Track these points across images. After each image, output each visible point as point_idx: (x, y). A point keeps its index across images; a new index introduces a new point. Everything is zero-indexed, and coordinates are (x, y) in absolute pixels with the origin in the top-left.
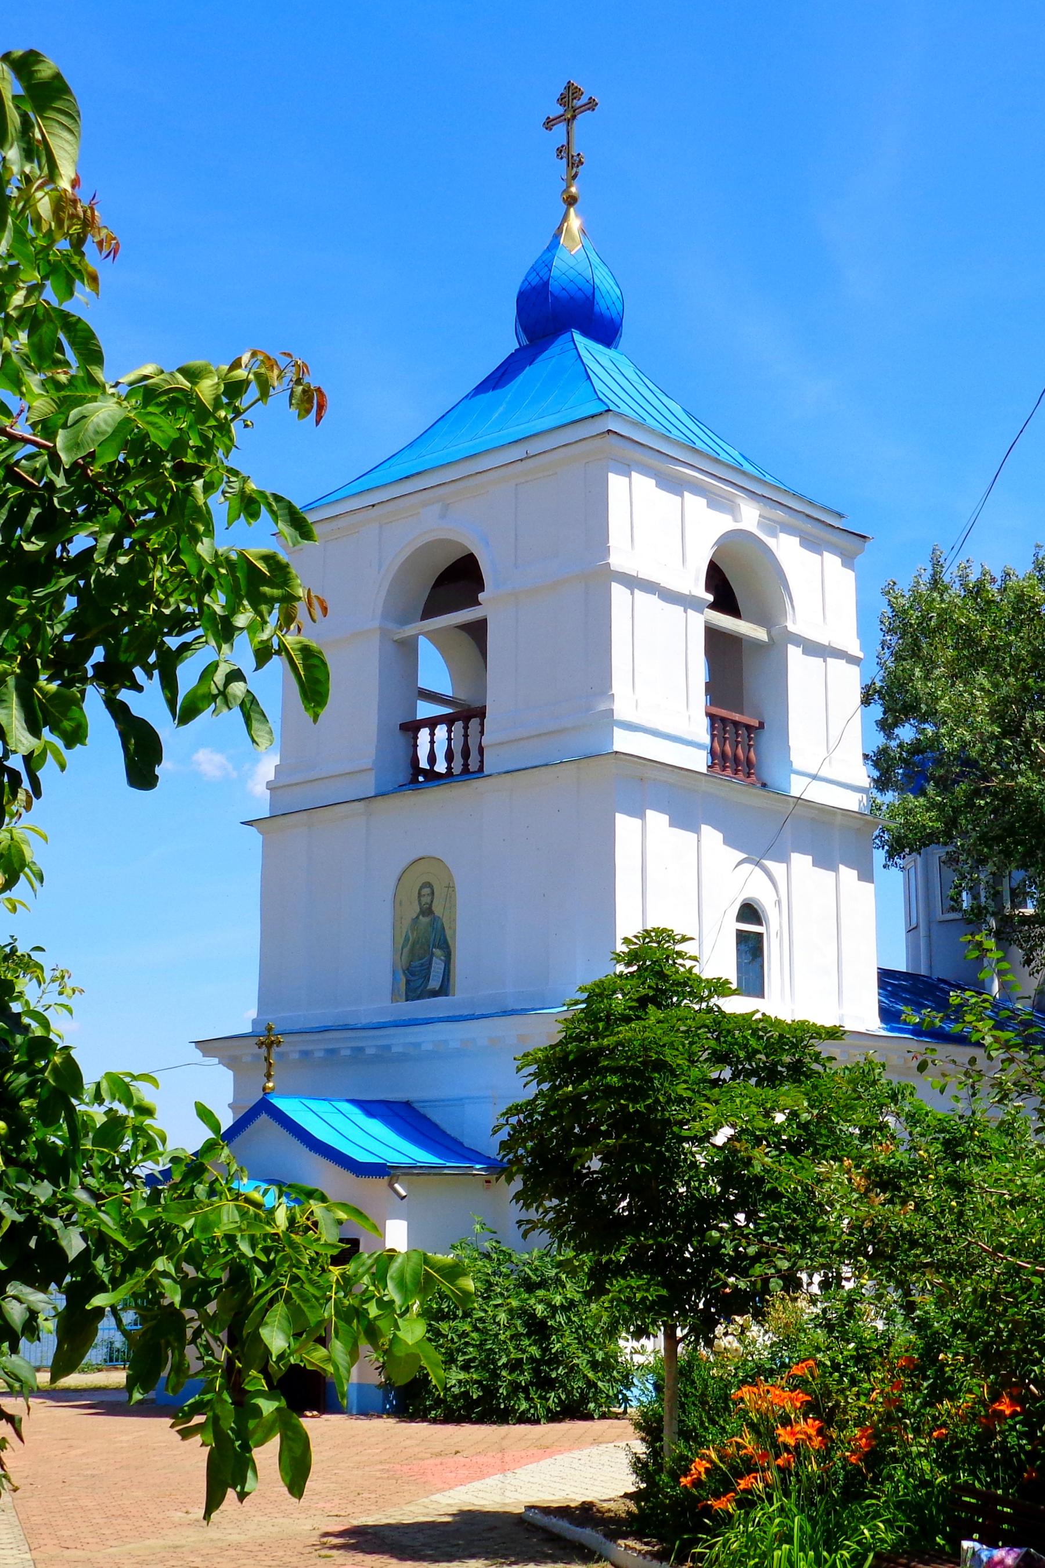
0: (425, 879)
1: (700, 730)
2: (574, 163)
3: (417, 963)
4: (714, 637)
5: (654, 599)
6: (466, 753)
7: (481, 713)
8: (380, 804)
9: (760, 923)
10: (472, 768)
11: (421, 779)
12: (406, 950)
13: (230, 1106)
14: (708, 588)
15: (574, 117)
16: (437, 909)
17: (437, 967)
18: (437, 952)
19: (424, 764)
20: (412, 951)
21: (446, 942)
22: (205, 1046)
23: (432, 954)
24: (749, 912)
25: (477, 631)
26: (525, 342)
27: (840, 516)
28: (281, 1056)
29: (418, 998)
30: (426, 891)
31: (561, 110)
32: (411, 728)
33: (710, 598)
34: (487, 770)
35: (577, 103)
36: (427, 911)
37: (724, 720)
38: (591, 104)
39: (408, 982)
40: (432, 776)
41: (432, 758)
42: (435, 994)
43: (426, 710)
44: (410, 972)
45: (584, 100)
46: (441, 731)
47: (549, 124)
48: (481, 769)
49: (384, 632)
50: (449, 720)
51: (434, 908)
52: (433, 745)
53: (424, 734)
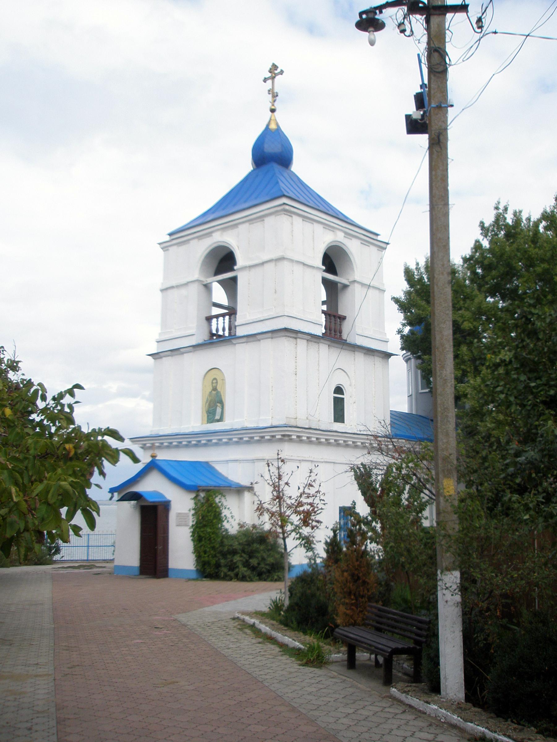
2: (275, 96)
9: (343, 394)
10: (232, 334)
12: (207, 404)
13: (108, 427)
15: (275, 77)
16: (219, 388)
17: (219, 410)
20: (209, 405)
23: (217, 406)
24: (339, 390)
25: (234, 280)
26: (255, 167)
29: (212, 422)
31: (269, 75)
32: (209, 319)
35: (276, 72)
36: (215, 389)
37: (330, 315)
38: (282, 72)
39: (208, 416)
41: (217, 330)
42: (218, 421)
43: (216, 311)
45: (279, 70)
46: (221, 319)
47: (265, 80)
50: (223, 315)
51: (218, 388)
53: (214, 320)
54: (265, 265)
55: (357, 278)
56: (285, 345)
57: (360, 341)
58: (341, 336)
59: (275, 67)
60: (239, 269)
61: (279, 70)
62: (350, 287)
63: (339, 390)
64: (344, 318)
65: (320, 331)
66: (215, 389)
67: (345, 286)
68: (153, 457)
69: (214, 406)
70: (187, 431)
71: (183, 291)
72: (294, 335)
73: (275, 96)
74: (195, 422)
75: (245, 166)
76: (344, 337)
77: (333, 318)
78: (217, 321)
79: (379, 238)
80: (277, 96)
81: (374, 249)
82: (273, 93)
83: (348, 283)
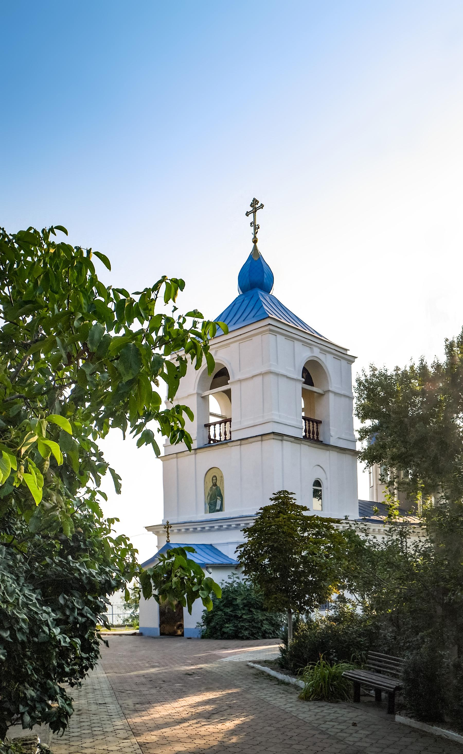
0: (214, 475)
5: (285, 379)
6: (225, 434)
7: (230, 420)
8: (198, 451)
11: (212, 442)
12: (209, 497)
14: (303, 377)
15: (256, 211)
16: (218, 484)
17: (219, 502)
18: (218, 497)
19: (212, 437)
21: (221, 494)
22: (149, 528)
23: (217, 498)
25: (228, 393)
26: (241, 293)
27: (346, 350)
28: (172, 531)
30: (214, 478)
31: (251, 209)
32: (208, 426)
33: (304, 380)
34: (232, 440)
35: (257, 206)
36: (215, 485)
39: (210, 507)
40: (214, 441)
41: (215, 436)
42: (218, 511)
43: (212, 420)
44: (210, 504)
45: (259, 205)
46: (217, 426)
48: (230, 439)
49: (198, 394)
50: (220, 423)
52: (216, 432)
53: (212, 427)
54: (254, 378)
55: (330, 389)
56: (273, 445)
57: (333, 442)
58: (317, 438)
59: (255, 201)
60: (232, 383)
61: (259, 205)
62: (325, 396)
66: (215, 485)
67: (321, 395)
72: (280, 438)
73: (255, 227)
75: (232, 292)
76: (321, 439)
77: (311, 422)
78: (215, 428)
79: (349, 353)
80: (258, 228)
81: (344, 363)
82: (255, 226)
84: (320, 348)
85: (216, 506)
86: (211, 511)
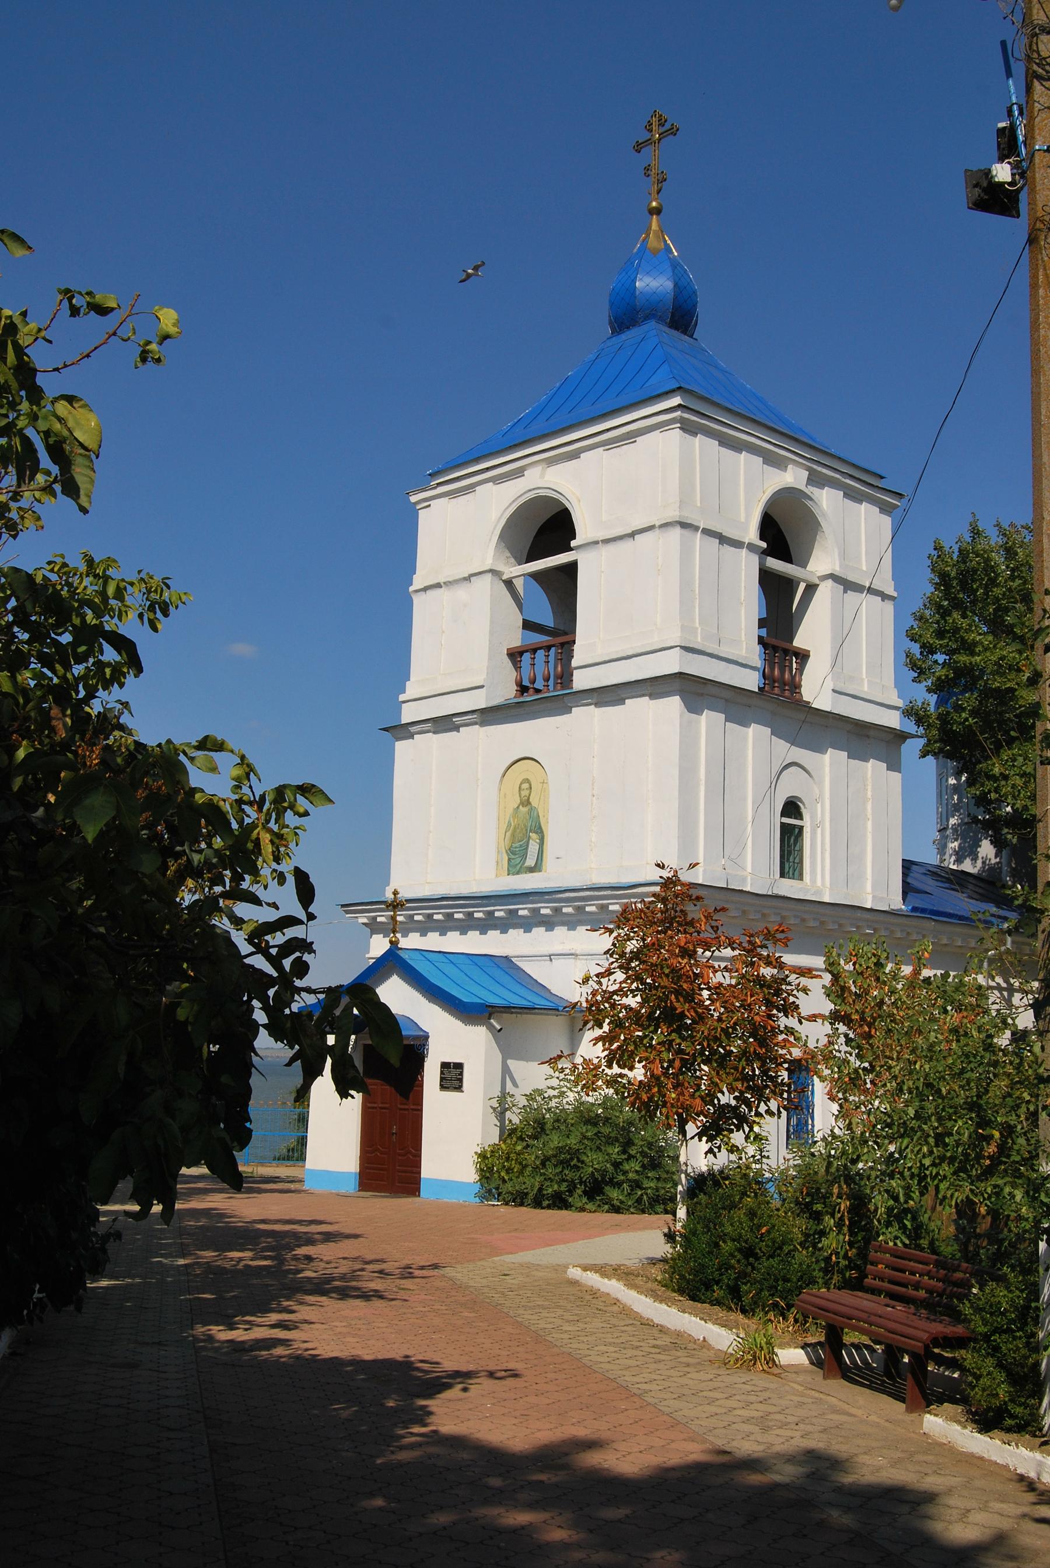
1: (754, 654)
3: (517, 845)
4: (767, 578)
9: (802, 819)
12: (509, 834)
14: (762, 538)
17: (533, 848)
18: (533, 835)
20: (513, 835)
21: (540, 828)
24: (792, 808)
29: (518, 873)
30: (525, 786)
33: (764, 545)
36: (526, 802)
37: (775, 649)
38: (673, 131)
39: (509, 860)
42: (531, 870)
44: (511, 851)
45: (668, 126)
46: (541, 654)
47: (639, 147)
53: (527, 656)
61: (668, 126)
63: (792, 808)
64: (803, 656)
65: (751, 681)
68: (394, 944)
69: (524, 839)
70: (465, 891)
71: (462, 593)
74: (482, 873)
83: (817, 581)
84: (809, 469)
85: (524, 856)
86: (513, 870)
